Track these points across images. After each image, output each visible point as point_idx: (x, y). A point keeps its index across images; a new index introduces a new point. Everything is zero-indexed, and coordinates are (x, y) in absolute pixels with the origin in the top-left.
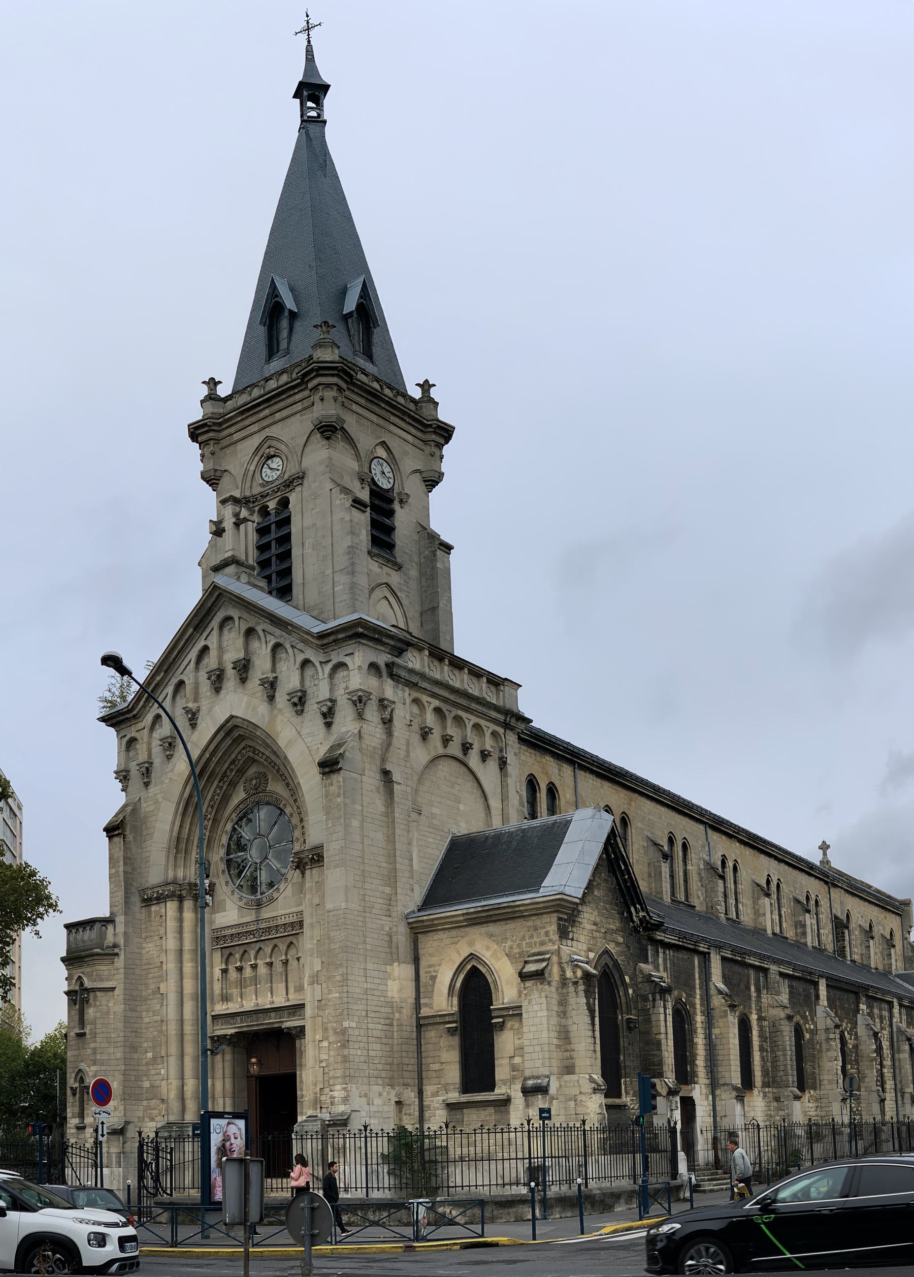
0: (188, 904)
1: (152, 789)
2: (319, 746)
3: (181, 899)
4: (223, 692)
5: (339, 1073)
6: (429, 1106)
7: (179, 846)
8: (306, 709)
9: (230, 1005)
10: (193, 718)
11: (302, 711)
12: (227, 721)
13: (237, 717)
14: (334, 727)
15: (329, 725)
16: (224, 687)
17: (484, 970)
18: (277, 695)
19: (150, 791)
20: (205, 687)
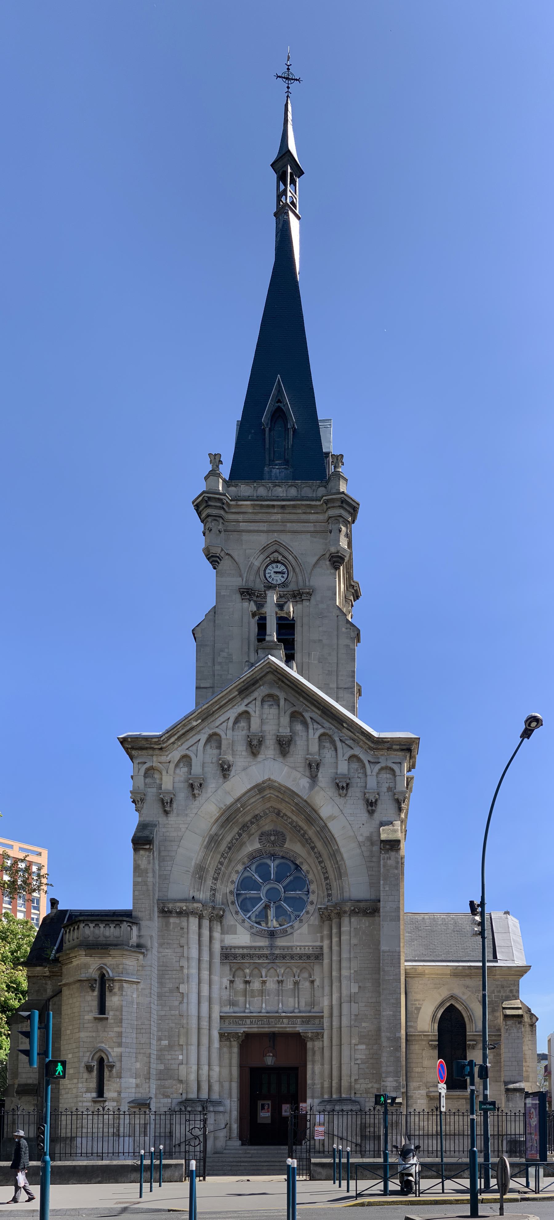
0: (206, 923)
1: (172, 819)
2: (361, 826)
3: (201, 917)
4: (261, 757)
5: (391, 1069)
6: (412, 1097)
7: (200, 872)
8: (349, 794)
9: (236, 1009)
10: (225, 770)
11: (346, 795)
12: (264, 782)
13: (275, 782)
14: (376, 815)
15: (371, 813)
16: (262, 752)
17: (460, 1008)
18: (320, 775)
19: (169, 819)
20: (241, 748)
